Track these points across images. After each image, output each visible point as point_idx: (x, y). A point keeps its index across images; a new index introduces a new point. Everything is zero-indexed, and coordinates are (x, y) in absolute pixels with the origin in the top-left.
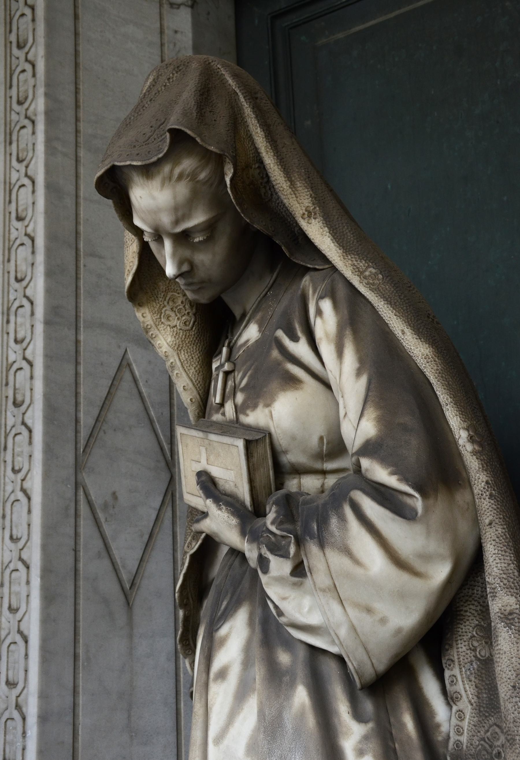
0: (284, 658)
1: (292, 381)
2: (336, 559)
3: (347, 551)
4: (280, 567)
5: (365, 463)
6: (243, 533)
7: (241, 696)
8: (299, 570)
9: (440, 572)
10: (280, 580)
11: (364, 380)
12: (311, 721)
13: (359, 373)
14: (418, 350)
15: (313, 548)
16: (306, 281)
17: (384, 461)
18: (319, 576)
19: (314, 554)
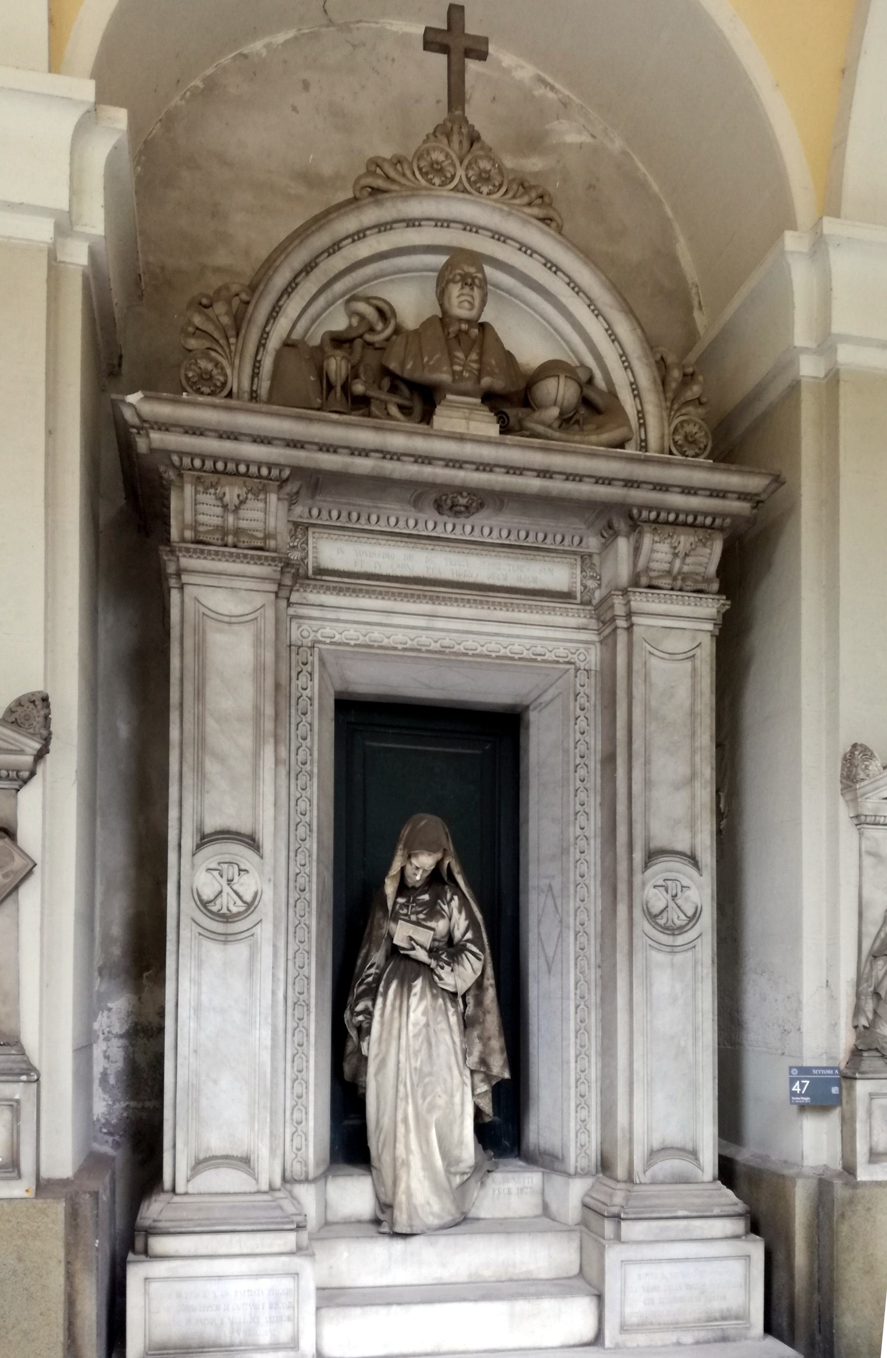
0: (435, 991)
1: (443, 917)
2: (461, 968)
3: (463, 966)
4: (448, 968)
5: (469, 945)
6: (430, 957)
7: (421, 998)
8: (452, 970)
9: (479, 973)
10: (447, 972)
11: (467, 922)
12: (443, 1007)
13: (466, 919)
14: (479, 916)
15: (456, 965)
16: (447, 887)
17: (475, 945)
18: (456, 972)
19: (456, 967)
